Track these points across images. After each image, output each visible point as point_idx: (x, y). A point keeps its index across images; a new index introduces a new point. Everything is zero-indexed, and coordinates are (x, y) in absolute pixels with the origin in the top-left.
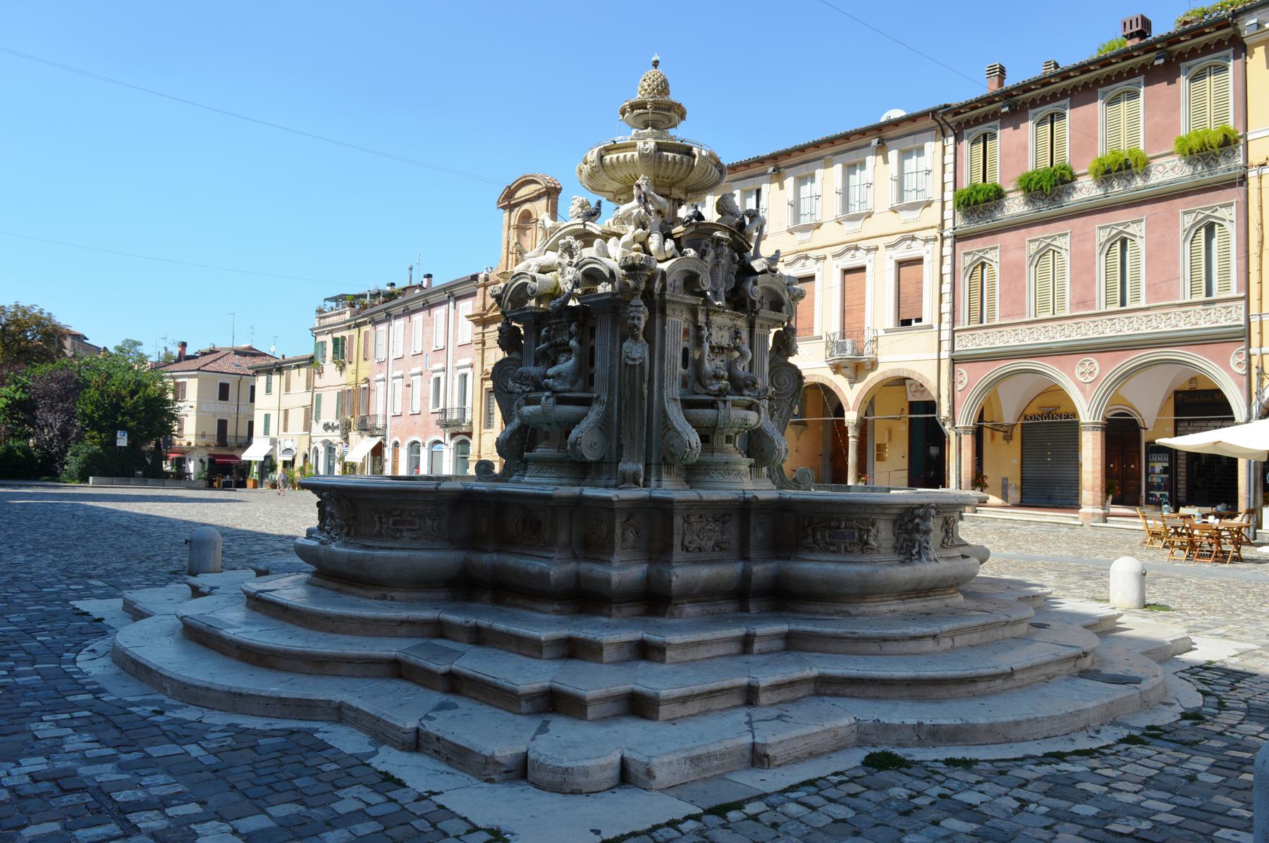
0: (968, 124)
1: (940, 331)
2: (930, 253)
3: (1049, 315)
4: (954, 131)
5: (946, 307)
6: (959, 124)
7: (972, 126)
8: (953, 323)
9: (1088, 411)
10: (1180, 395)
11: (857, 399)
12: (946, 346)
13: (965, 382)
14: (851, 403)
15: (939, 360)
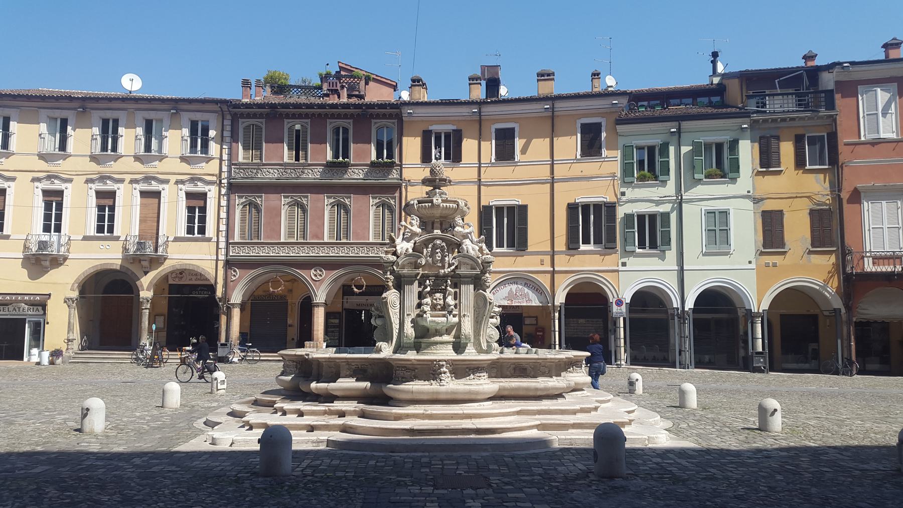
0: (242, 116)
1: (218, 242)
2: (212, 193)
3: (294, 240)
4: (232, 117)
5: (223, 227)
6: (236, 114)
7: (245, 118)
8: (227, 237)
9: (320, 296)
10: (346, 288)
11: (151, 282)
12: (223, 251)
13: (237, 276)
14: (145, 286)
15: (217, 260)
